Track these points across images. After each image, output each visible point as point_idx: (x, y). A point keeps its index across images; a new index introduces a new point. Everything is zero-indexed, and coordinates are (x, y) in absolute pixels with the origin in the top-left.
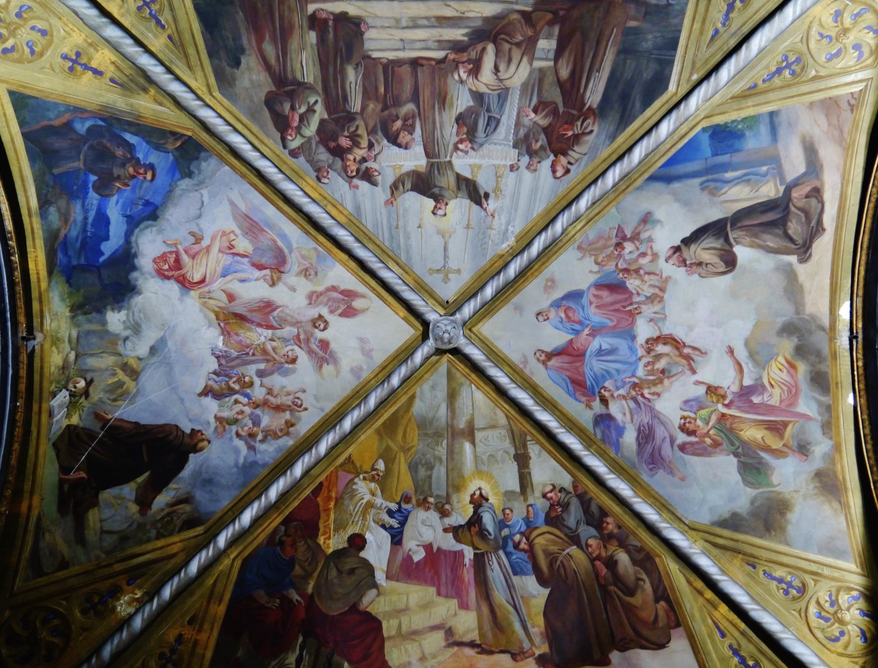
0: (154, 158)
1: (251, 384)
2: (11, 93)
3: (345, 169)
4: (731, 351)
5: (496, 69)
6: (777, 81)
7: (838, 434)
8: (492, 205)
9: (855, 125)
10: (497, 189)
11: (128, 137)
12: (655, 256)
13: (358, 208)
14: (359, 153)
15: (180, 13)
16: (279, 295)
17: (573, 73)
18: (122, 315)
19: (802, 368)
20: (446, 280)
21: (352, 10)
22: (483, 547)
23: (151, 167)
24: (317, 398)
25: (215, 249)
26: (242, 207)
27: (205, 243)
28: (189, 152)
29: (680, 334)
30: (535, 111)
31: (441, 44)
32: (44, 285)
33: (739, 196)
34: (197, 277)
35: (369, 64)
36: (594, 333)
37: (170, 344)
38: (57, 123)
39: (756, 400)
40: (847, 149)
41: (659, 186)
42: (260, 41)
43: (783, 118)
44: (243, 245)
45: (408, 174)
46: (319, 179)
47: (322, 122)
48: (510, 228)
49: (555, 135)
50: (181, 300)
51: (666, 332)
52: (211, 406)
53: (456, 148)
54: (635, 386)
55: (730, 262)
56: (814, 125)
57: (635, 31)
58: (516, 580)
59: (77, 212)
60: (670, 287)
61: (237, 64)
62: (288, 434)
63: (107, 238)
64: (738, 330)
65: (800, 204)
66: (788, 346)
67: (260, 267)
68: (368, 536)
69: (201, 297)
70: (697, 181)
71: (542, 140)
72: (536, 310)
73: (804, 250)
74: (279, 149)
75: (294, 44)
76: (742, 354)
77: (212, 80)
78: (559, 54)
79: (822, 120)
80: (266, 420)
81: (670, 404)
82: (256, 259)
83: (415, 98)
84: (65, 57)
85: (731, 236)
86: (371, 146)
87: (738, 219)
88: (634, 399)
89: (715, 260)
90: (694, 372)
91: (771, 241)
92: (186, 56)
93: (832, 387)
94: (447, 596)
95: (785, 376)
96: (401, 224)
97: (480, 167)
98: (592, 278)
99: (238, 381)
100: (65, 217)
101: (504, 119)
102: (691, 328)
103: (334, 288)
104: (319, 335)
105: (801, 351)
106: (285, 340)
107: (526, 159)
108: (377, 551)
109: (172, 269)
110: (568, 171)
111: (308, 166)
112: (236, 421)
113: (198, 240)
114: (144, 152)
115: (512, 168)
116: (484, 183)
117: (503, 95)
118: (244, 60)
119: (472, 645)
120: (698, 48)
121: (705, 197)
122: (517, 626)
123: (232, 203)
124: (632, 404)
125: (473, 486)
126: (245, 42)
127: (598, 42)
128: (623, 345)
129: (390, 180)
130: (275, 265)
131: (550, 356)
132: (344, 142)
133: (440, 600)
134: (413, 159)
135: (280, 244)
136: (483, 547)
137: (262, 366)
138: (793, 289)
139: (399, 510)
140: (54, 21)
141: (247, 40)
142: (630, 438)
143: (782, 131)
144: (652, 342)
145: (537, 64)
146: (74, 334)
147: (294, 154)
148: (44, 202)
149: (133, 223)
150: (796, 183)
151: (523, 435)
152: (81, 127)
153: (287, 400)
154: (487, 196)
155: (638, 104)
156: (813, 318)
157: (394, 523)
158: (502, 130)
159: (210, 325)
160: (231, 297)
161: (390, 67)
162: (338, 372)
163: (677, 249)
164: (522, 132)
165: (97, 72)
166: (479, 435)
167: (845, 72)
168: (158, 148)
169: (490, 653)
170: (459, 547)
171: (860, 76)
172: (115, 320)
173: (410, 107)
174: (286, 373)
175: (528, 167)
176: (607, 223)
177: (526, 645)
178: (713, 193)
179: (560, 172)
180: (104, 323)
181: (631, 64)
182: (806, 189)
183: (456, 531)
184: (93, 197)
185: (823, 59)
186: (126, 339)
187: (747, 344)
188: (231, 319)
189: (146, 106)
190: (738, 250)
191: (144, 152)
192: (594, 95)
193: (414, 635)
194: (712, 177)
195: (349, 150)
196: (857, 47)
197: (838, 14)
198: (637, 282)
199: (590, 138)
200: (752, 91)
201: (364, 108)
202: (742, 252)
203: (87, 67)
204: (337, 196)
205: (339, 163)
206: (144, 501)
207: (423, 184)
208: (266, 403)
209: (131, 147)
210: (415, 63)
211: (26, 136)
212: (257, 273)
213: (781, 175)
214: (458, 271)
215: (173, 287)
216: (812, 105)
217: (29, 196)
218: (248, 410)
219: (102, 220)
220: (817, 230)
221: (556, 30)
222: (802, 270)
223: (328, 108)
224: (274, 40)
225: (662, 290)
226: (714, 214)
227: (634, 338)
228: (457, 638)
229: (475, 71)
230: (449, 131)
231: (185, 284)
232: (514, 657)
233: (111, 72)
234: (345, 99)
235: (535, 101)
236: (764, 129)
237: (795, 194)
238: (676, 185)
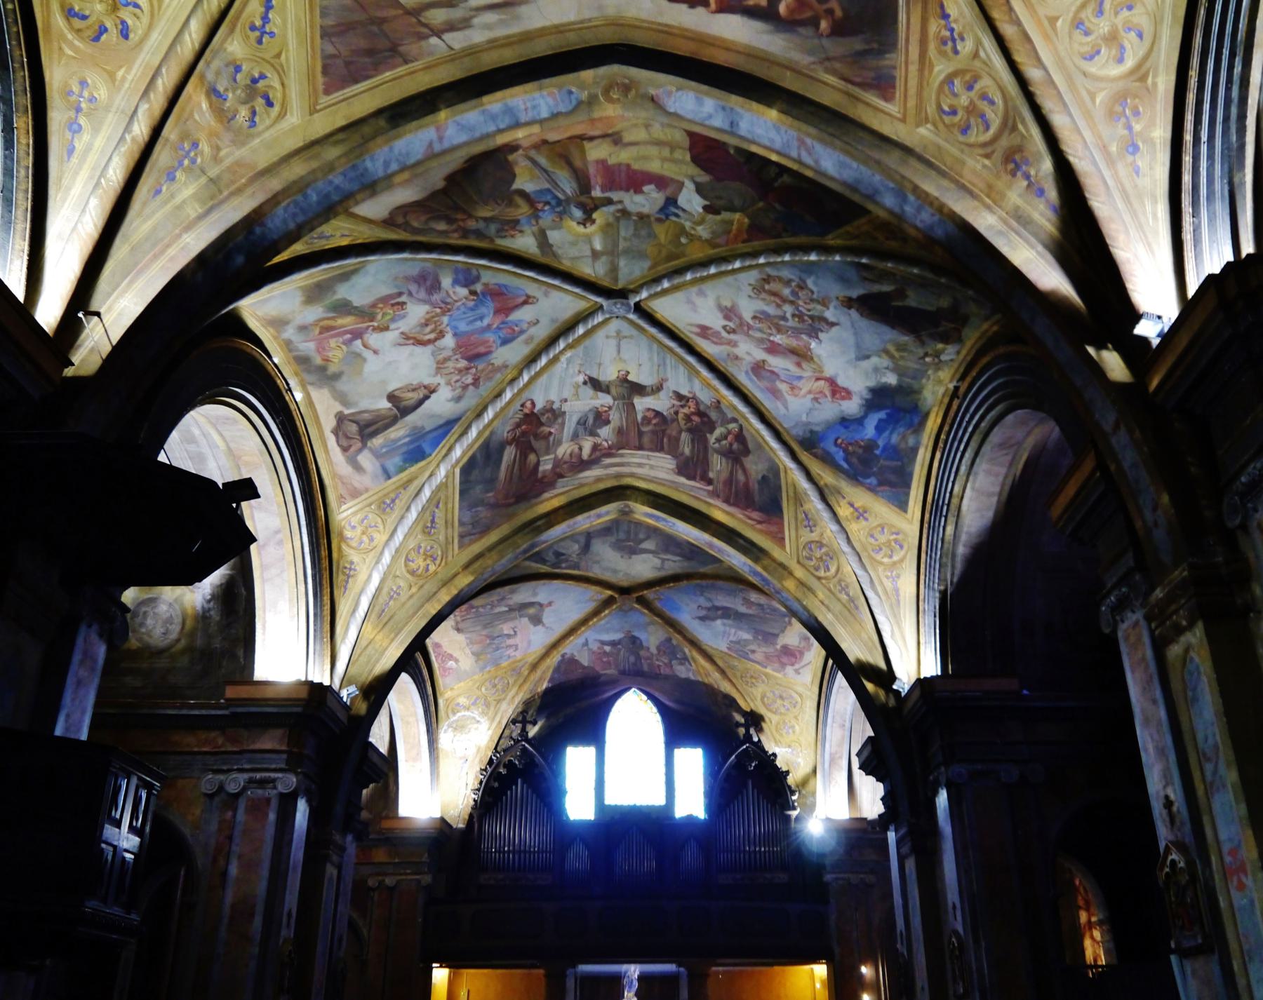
0: (833, 449)
1: (793, 315)
2: (905, 511)
3: (697, 404)
4: (376, 352)
5: (580, 449)
6: (393, 495)
7: (280, 346)
8: (581, 378)
9: (335, 488)
10: (577, 386)
11: (845, 466)
12: (448, 383)
13: (690, 380)
14: (686, 410)
15: (792, 514)
16: (760, 355)
17: (526, 457)
18: (884, 380)
20: (618, 332)
21: (683, 480)
22: (583, 199)
23: (836, 444)
24: (739, 289)
25: (804, 391)
26: (779, 404)
27: (812, 396)
28: (808, 444)
29: (419, 350)
30: (550, 433)
31: (622, 455)
32: (935, 409)
33: (398, 432)
34: (822, 383)
35: (674, 451)
36: (489, 326)
37: (853, 356)
38: (887, 488)
39: (349, 336)
40: (335, 475)
42: (746, 484)
43: (382, 478)
44: (783, 387)
45: (648, 395)
47: (712, 431)
49: (533, 427)
50: (837, 375)
51: (430, 348)
52: (830, 314)
53: (610, 408)
54: (449, 310)
55: (392, 397)
56: (358, 481)
57: (487, 491)
58: (547, 186)
59: (895, 439)
60: (433, 371)
61: (764, 477)
62: (769, 276)
63: (880, 421)
64: (372, 365)
65: (352, 442)
67: (773, 372)
68: (701, 210)
70: (428, 429)
71: (544, 419)
72: (539, 326)
73: (341, 418)
74: (745, 424)
75: (725, 475)
76: (367, 354)
77: (782, 475)
78: (538, 464)
79: (357, 485)
80: (786, 292)
81: (416, 312)
83: (640, 434)
84: (866, 519)
85: (395, 411)
86: (676, 413)
87: (393, 421)
88: (446, 303)
90: (402, 333)
91: (366, 416)
92: (795, 492)
93: (292, 361)
94: (620, 165)
95: (330, 354)
96: (656, 368)
98: (494, 355)
99: (803, 321)
100: (904, 437)
101: (573, 425)
102: (411, 355)
103: (716, 343)
104: (731, 324)
105: (322, 369)
106: (760, 330)
107: (555, 406)
108: (691, 201)
109: (838, 391)
110: (522, 405)
112: (812, 300)
113: (816, 399)
114: (839, 456)
115: (566, 401)
116: (589, 391)
117: (575, 437)
118: (760, 477)
119: (591, 139)
120: (447, 497)
121: (419, 424)
122: (543, 161)
123: (786, 408)
124: (449, 300)
125: (591, 229)
126: (756, 486)
127: (511, 478)
128: (463, 327)
129: (662, 394)
130: (758, 368)
131: (525, 302)
132: (696, 419)
133: (625, 161)
134: (642, 404)
136: (583, 199)
137: (782, 323)
138: (343, 399)
139: (667, 216)
140: (863, 539)
141: (755, 487)
142: (446, 282)
143: (379, 471)
144: (441, 335)
145: (552, 456)
146: (924, 381)
147: (734, 420)
148: (915, 450)
149: (860, 421)
150: (360, 450)
151: (543, 253)
152: (873, 480)
153: (763, 295)
154: (585, 383)
155: (478, 456)
156: (321, 387)
157: (673, 210)
158: (575, 419)
159: (819, 357)
160: (799, 365)
161: (660, 449)
162: (718, 298)
163: (433, 391)
164: (560, 420)
165: (852, 505)
166: (589, 253)
167: (355, 513)
168: (828, 453)
169: (570, 138)
170: (607, 194)
171: (345, 514)
172: (891, 379)
173: (645, 429)
174: (763, 312)
176: (486, 389)
177: (533, 153)
178: (415, 428)
179: (528, 404)
181: (488, 473)
182: (352, 449)
183: (609, 202)
184: (881, 443)
185: (370, 516)
186: (887, 368)
187: (365, 360)
188: (801, 356)
189: (827, 477)
190: (389, 405)
191: (839, 456)
192: (509, 453)
193: (659, 143)
195: (693, 414)
196: (354, 527)
197: (372, 539)
199: (508, 428)
200: (405, 485)
201: (680, 432)
202: (385, 404)
203: (856, 510)
204: (706, 390)
205: (702, 408)
206: (901, 294)
207: (638, 389)
208: (785, 301)
209: (846, 460)
210: (640, 448)
211: (908, 486)
213: (371, 450)
214: (607, 337)
215: (841, 382)
216: (367, 490)
217: (923, 456)
218: (801, 303)
219: (879, 428)
220: (336, 432)
221: (540, 475)
222: (338, 407)
223: (706, 441)
224: (737, 482)
225: (438, 369)
226: (412, 418)
227: (455, 335)
228: (608, 140)
229: (595, 447)
230: (615, 418)
231: (832, 382)
232: (545, 142)
233: (843, 503)
234: (693, 441)
235: (551, 439)
236: (391, 469)
237: (359, 445)
238: (441, 422)
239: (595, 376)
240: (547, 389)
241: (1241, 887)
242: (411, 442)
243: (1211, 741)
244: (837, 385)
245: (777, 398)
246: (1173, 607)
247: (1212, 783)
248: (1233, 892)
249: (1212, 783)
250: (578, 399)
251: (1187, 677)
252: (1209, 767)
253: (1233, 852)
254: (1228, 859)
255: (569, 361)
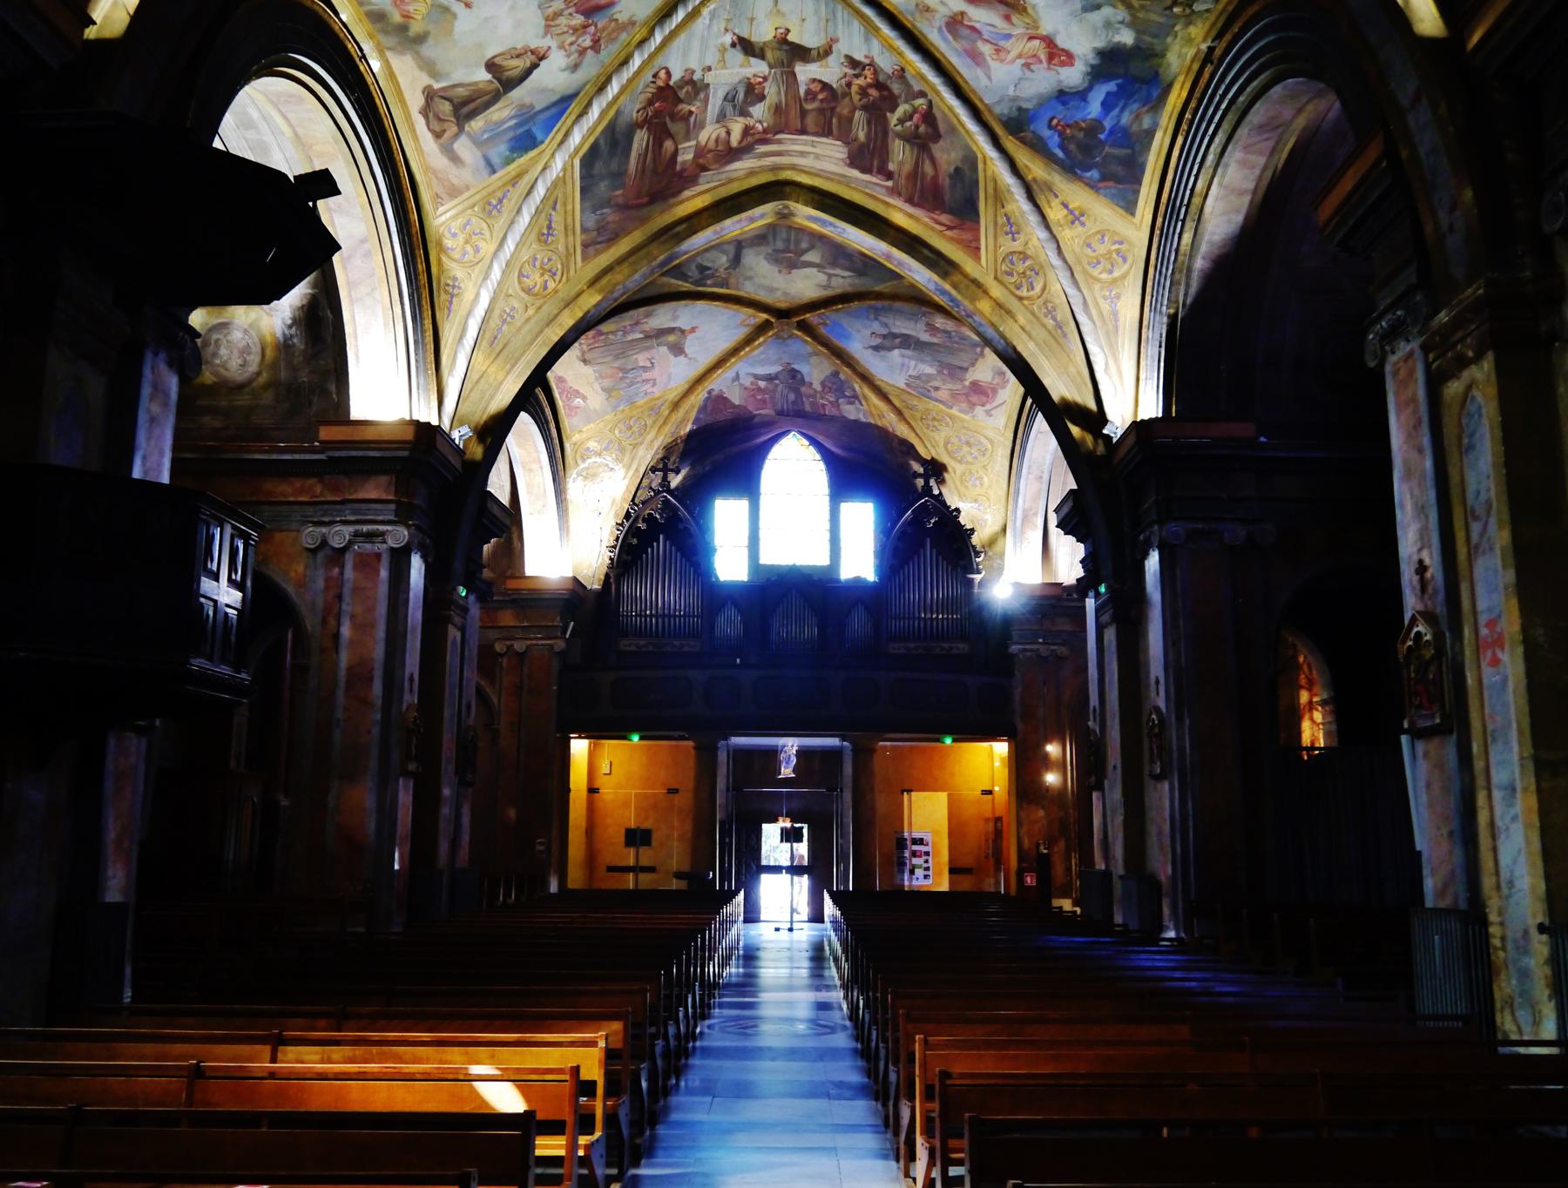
0: (1046, 133)
2: (1133, 214)
5: (728, 133)
6: (499, 194)
8: (728, 39)
9: (429, 185)
10: (723, 50)
11: (1060, 154)
12: (561, 47)
13: (867, 40)
14: (861, 81)
15: (990, 218)
17: (661, 146)
18: (1117, 39)
19: (397, 18)
21: (855, 173)
23: (1050, 127)
27: (1022, 61)
28: (1015, 126)
30: (691, 113)
31: (779, 142)
32: (1181, 78)
33: (501, 112)
34: (1036, 42)
35: (845, 136)
37: (1079, 6)
38: (1111, 184)
40: (427, 169)
41: (570, 91)
42: (935, 178)
43: (485, 172)
44: (986, 49)
46: (903, 70)
47: (893, 110)
48: (707, 21)
49: (669, 104)
50: (1057, 32)
53: (765, 79)
55: (491, 66)
56: (457, 176)
57: (617, 189)
59: (1126, 119)
60: (542, 31)
61: (957, 170)
63: (1108, 94)
65: (446, 125)
66: (416, 28)
67: (973, 29)
69: (1037, 28)
70: (538, 108)
71: (682, 94)
73: (430, 95)
74: (936, 100)
75: (908, 168)
77: (980, 166)
78: (676, 153)
79: (455, 181)
82: (975, 36)
83: (803, 113)
84: (1083, 224)
86: (849, 85)
87: (495, 97)
89: (505, 63)
91: (461, 91)
92: (995, 190)
93: (364, 18)
95: (411, 8)
96: (823, 23)
97: (742, 66)
98: (617, 8)
100: (1138, 117)
101: (719, 102)
105: (403, 29)
109: (1057, 55)
110: (655, 76)
111: (912, 82)
113: (1027, 66)
114: (1053, 141)
115: (709, 69)
116: (737, 56)
117: (722, 117)
118: (952, 169)
120: (565, 194)
121: (527, 101)
123: (989, 78)
126: (947, 181)
127: (643, 172)
129: (831, 59)
130: (955, 23)
132: (873, 92)
134: (806, 73)
135: (950, 37)
138: (430, 68)
140: (1078, 250)
141: (945, 182)
143: (482, 163)
145: (693, 143)
146: (1169, 40)
147: (922, 94)
148: (1150, 134)
149: (1082, 95)
150: (456, 136)
152: (1094, 174)
154: (733, 45)
155: (602, 142)
156: (402, 53)
158: (721, 94)
160: (1007, 18)
161: (826, 131)
163: (542, 58)
164: (702, 95)
165: (1065, 206)
167: (454, 218)
168: (1040, 139)
171: (443, 218)
172: (1127, 37)
173: (809, 107)
175: (693, 72)
176: (609, 53)
178: (523, 106)
179: (662, 74)
180: (1137, 39)
181: (614, 167)
182: (446, 135)
184: (1108, 124)
185: (474, 220)
186: (1122, 22)
187: (455, 16)
189: (1036, 169)
190: (488, 77)
191: (1053, 141)
192: (641, 139)
194: (527, 116)
195: (870, 86)
196: (455, 235)
197: (477, 250)
198: (573, 23)
199: (638, 106)
200: (514, 181)
201: (853, 111)
202: (483, 76)
203: (1072, 212)
205: (881, 78)
207: (800, 53)
209: (1062, 147)
210: (803, 132)
211: (1138, 181)
212: (977, 26)
213: (469, 135)
215: (1062, 42)
216: (468, 188)
217: (1160, 141)
219: (1107, 105)
220: (426, 111)
221: (678, 167)
222: (426, 80)
223: (885, 122)
224: (923, 174)
225: (548, 27)
226: (517, 94)
229: (747, 131)
230: (771, 90)
231: (1049, 41)
233: (1055, 203)
234: (869, 122)
235: (692, 119)
236: (496, 160)
237: (455, 129)
238: (555, 98)
239: (746, 36)
240: (685, 55)
241: (1495, 662)
242: (518, 125)
243: (1483, 497)
244: (1056, 46)
245: (978, 64)
246: (1460, 334)
247: (1477, 547)
248: (1484, 665)
249: (1477, 547)
250: (724, 67)
251: (1464, 421)
252: (1476, 527)
253: (1491, 624)
254: (1484, 631)
255: (713, 15)
